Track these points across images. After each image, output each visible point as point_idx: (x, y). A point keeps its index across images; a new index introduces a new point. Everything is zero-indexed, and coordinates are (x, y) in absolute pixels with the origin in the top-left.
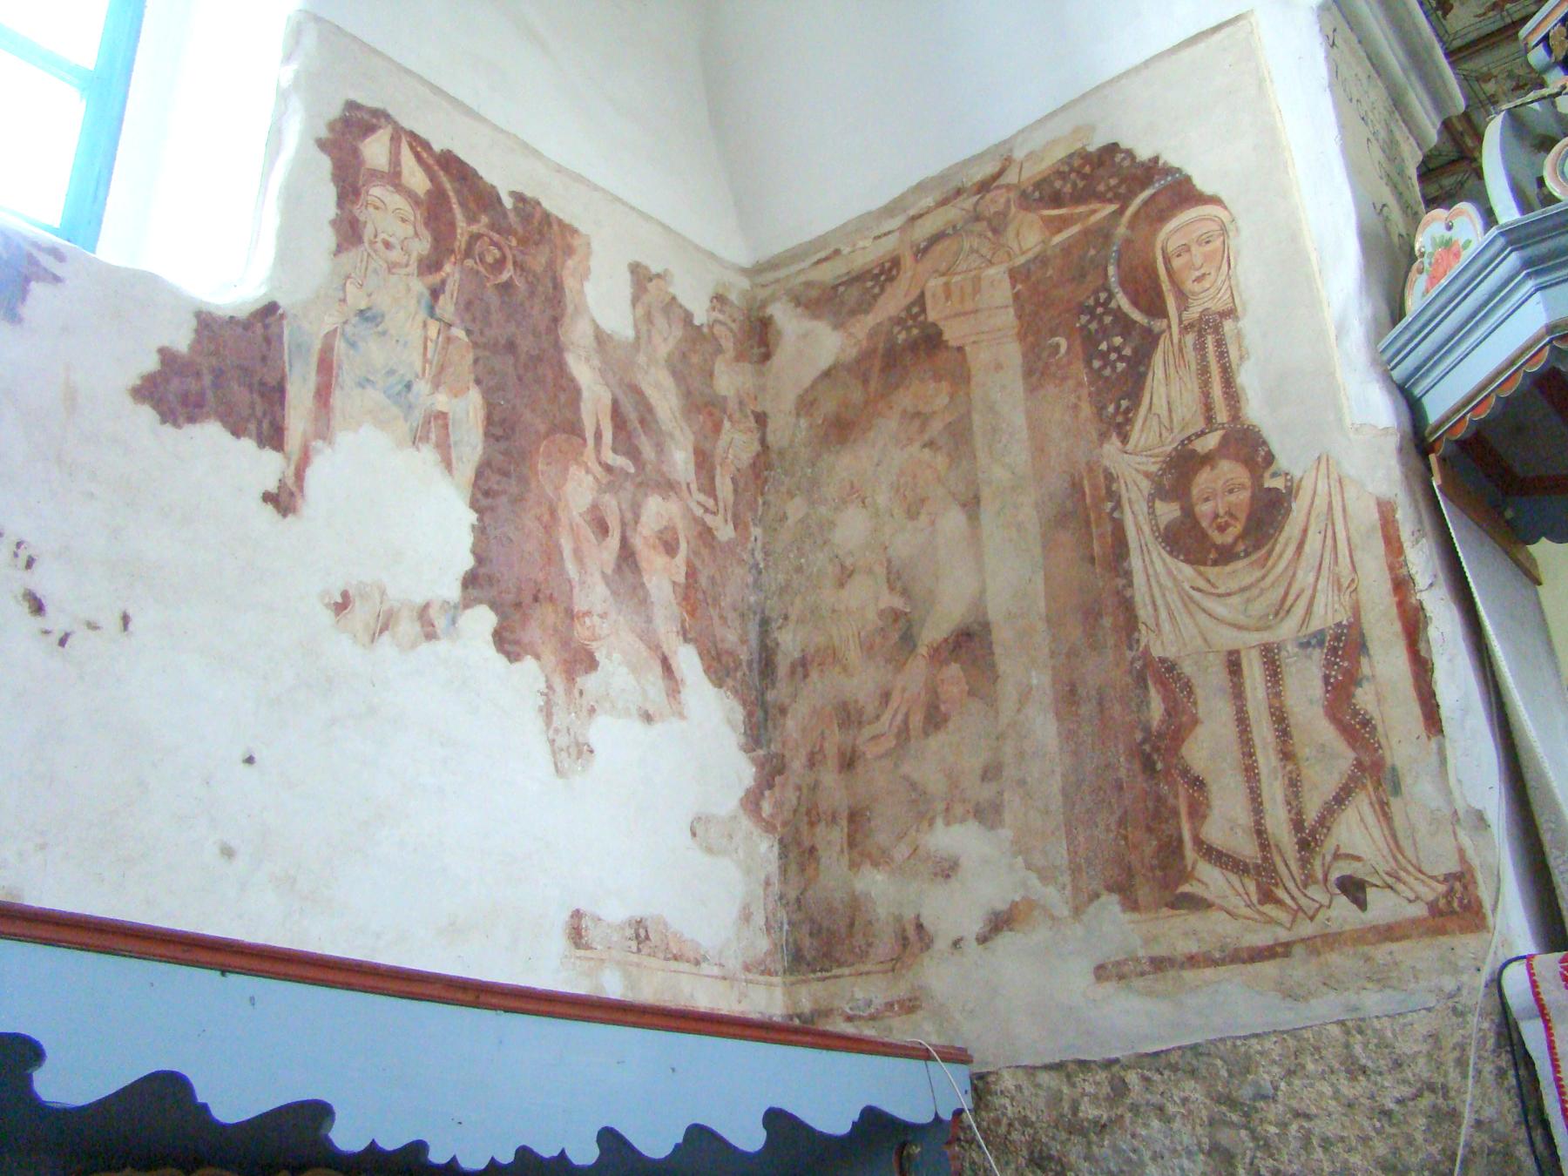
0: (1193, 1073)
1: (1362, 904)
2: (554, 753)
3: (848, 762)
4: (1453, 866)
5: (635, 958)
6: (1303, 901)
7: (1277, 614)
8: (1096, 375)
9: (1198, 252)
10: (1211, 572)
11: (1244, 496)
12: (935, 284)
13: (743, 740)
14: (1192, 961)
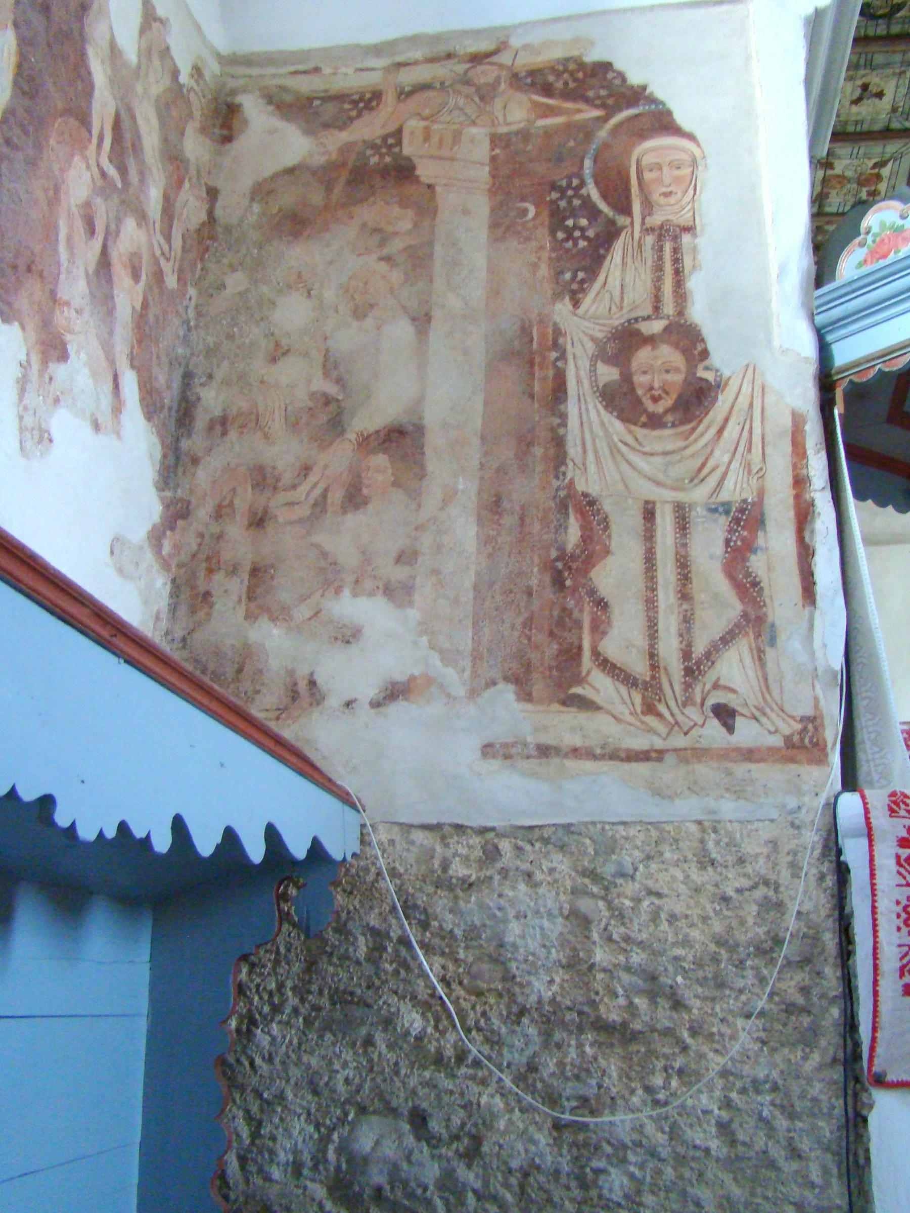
0: (562, 848)
1: (730, 729)
2: (21, 430)
6: (680, 718)
7: (692, 480)
8: (557, 245)
10: (640, 432)
11: (677, 378)
12: (414, 125)
14: (576, 752)
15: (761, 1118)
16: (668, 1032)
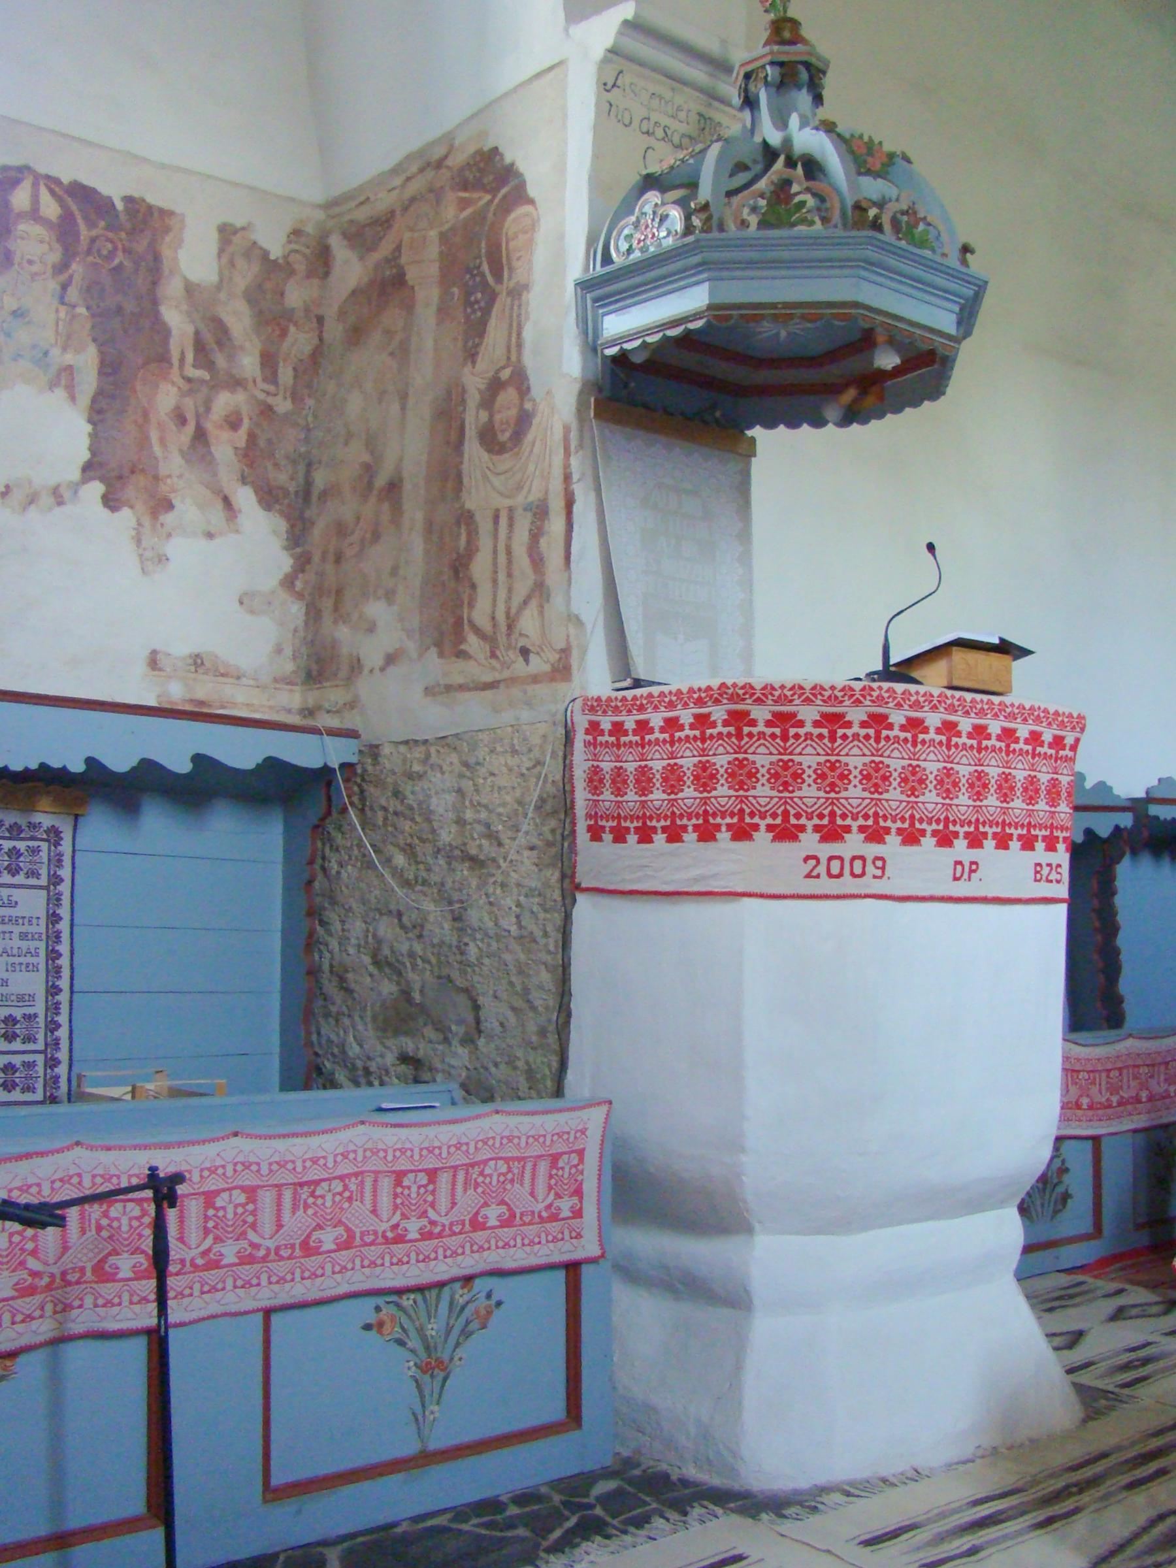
1: (527, 661)
2: (142, 562)
3: (339, 559)
4: (562, 645)
5: (193, 676)
6: (507, 658)
8: (468, 318)
9: (522, 238)
10: (495, 457)
13: (285, 543)
14: (462, 688)
15: (532, 912)
16: (494, 860)
